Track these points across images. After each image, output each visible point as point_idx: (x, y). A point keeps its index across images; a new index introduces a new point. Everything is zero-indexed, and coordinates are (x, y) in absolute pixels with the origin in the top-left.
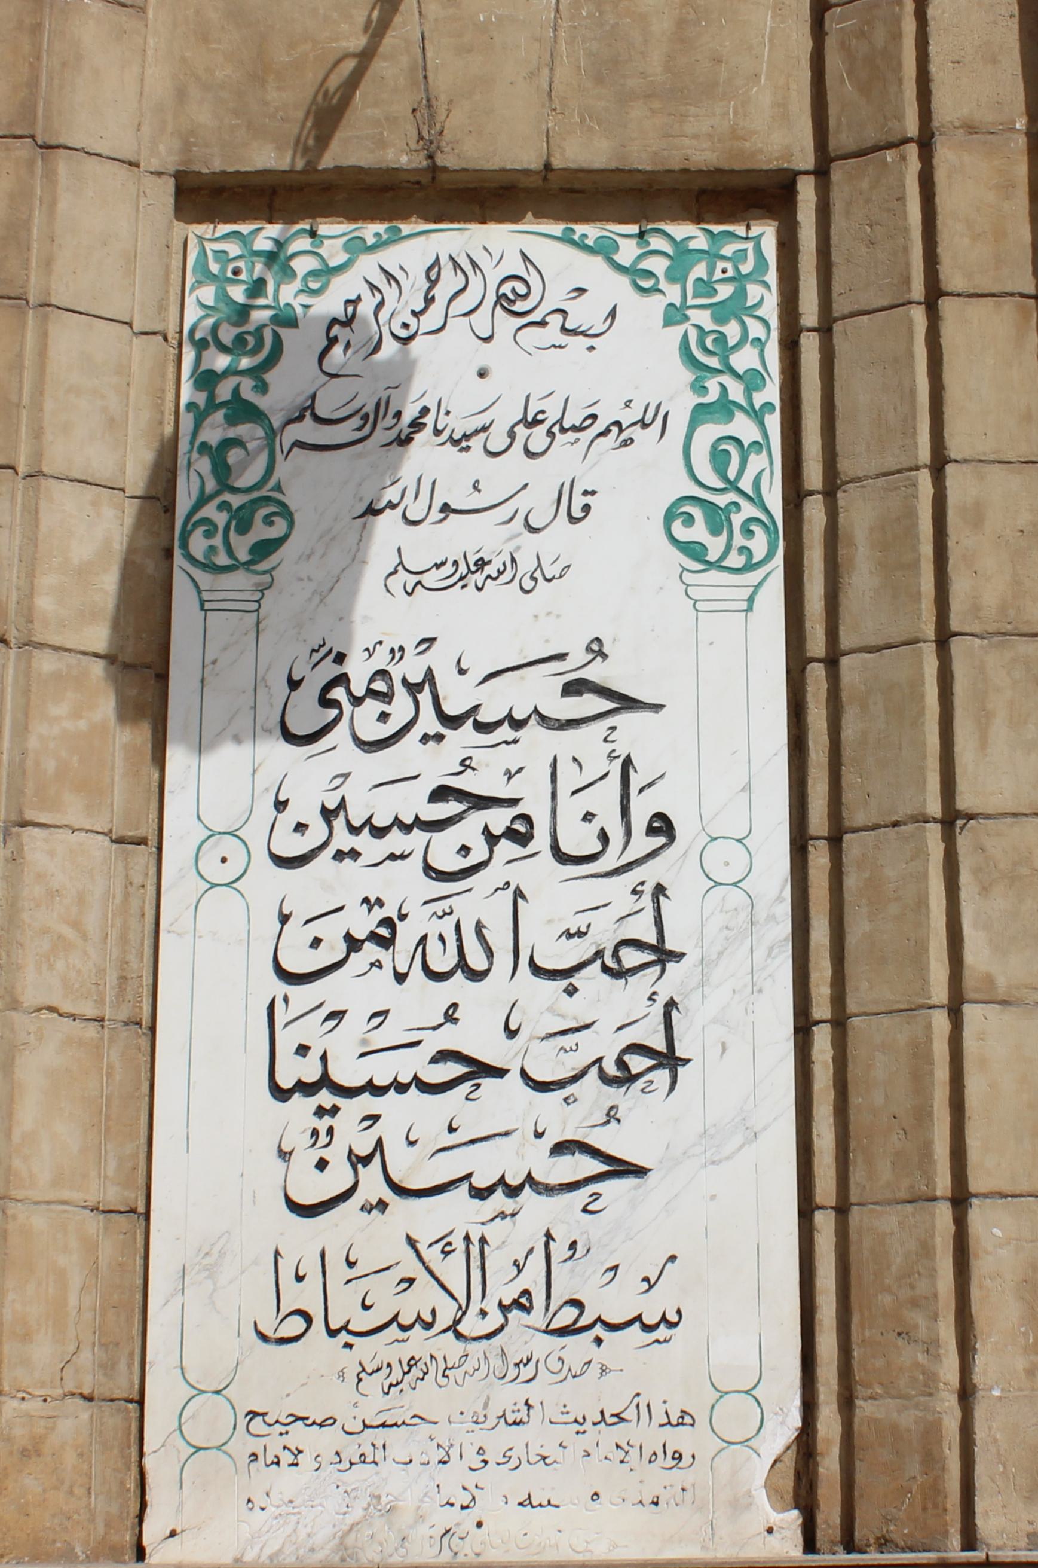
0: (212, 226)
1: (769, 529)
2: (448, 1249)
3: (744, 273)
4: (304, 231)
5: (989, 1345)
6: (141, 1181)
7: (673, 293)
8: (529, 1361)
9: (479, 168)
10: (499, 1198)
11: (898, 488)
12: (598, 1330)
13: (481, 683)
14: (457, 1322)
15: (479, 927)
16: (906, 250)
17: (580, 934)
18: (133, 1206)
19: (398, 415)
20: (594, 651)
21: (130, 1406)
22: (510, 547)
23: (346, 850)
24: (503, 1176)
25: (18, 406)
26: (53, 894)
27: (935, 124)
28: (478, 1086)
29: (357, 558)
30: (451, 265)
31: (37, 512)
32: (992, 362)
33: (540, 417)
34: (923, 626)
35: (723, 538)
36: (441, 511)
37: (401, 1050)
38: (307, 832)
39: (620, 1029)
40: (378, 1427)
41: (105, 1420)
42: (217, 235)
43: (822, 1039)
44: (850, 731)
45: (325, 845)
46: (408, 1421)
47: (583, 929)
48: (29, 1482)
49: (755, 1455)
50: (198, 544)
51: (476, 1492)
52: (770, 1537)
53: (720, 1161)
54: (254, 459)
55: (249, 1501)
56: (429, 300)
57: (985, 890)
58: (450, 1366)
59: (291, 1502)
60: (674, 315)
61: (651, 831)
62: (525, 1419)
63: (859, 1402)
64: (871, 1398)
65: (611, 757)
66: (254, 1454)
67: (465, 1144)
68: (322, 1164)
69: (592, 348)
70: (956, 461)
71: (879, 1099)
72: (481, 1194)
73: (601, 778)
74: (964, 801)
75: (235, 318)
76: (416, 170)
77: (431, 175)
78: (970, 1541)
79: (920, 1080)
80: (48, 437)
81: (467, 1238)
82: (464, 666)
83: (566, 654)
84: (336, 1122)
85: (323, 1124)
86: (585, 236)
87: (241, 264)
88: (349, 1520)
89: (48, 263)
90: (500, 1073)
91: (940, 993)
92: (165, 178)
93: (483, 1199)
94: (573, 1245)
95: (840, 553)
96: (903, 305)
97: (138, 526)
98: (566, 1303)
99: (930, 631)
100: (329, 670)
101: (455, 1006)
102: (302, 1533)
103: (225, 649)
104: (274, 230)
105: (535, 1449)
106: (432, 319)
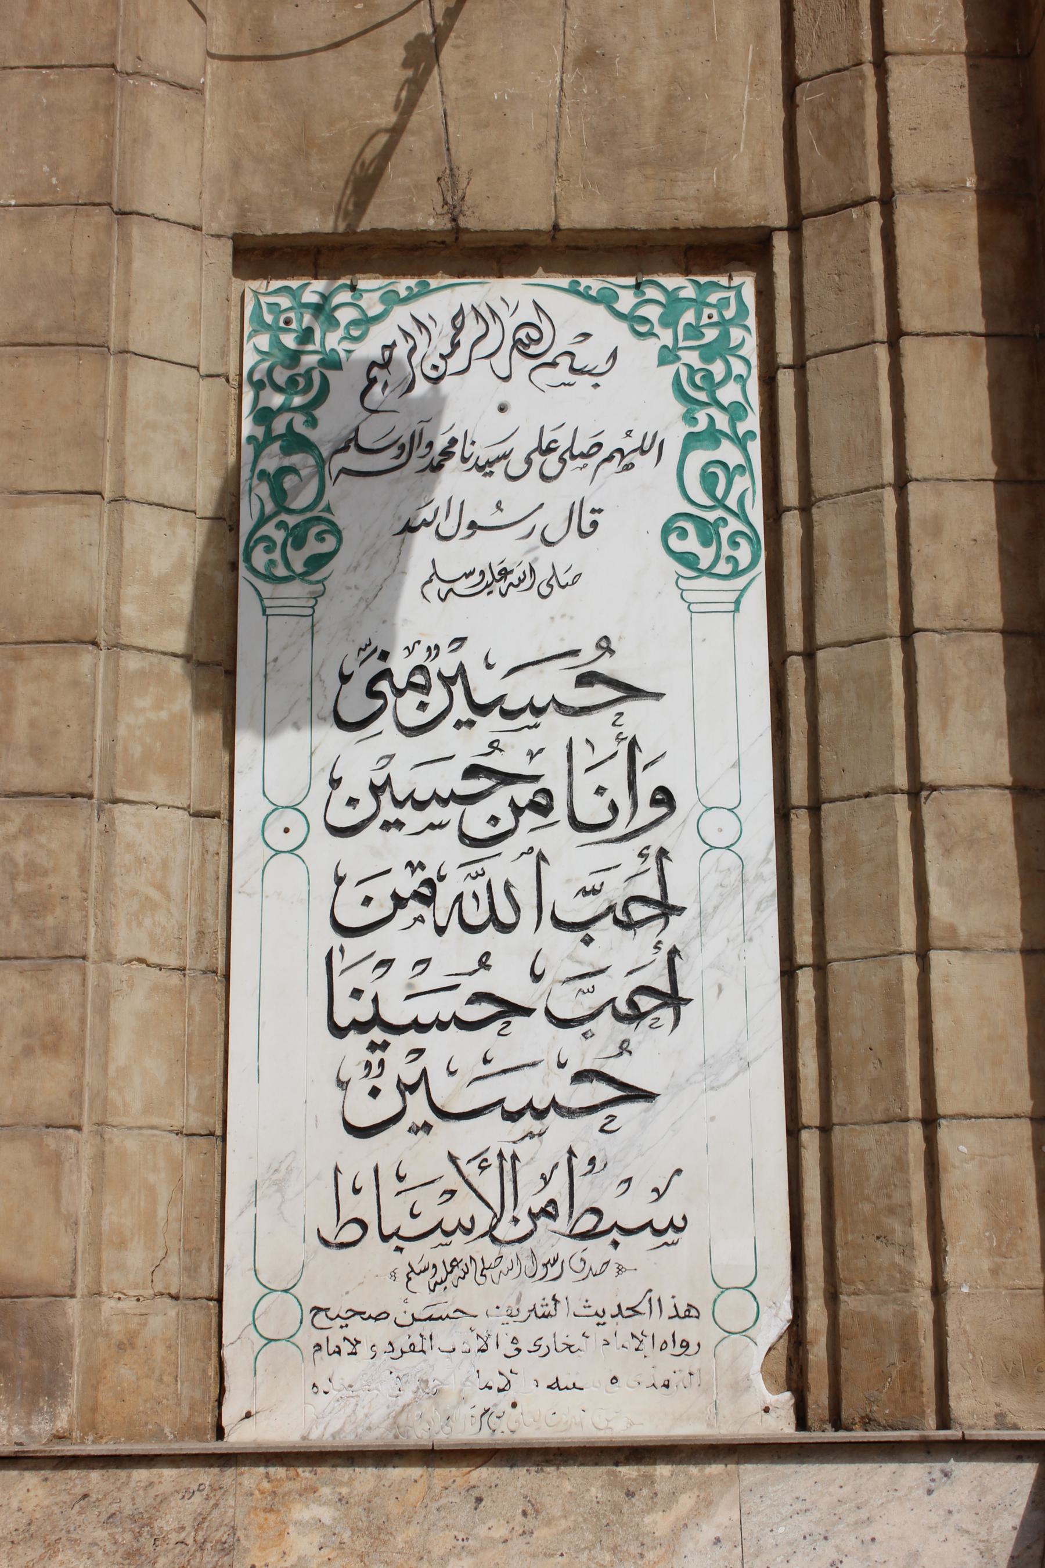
0: (265, 282)
1: (753, 541)
2: (484, 1164)
3: (727, 318)
4: (345, 285)
5: (958, 1248)
6: (218, 1108)
7: (666, 337)
8: (555, 1261)
9: (495, 229)
10: (527, 1122)
11: (866, 504)
12: (615, 1234)
13: (505, 676)
14: (493, 1228)
15: (508, 887)
16: (870, 295)
17: (595, 892)
18: (212, 1130)
19: (430, 445)
20: (603, 648)
21: (211, 1303)
22: (529, 558)
23: (392, 821)
24: (531, 1100)
25: (103, 439)
26: (141, 861)
27: (895, 184)
28: (509, 1023)
29: (397, 569)
30: (473, 314)
31: (121, 531)
32: (948, 392)
33: (553, 446)
34: (890, 624)
35: (713, 548)
36: (469, 528)
37: (442, 993)
38: (358, 806)
39: (630, 973)
40: (425, 1320)
41: (188, 1317)
42: (270, 289)
43: (805, 981)
44: (826, 715)
45: (374, 816)
46: (451, 1315)
47: (597, 887)
48: (123, 1371)
49: (752, 1344)
50: (260, 558)
51: (511, 1376)
52: (766, 1416)
53: (719, 1087)
54: (307, 483)
55: (314, 1385)
56: (455, 345)
57: (947, 852)
58: (487, 1266)
59: (351, 1386)
60: (667, 356)
61: (654, 802)
62: (553, 1313)
63: (843, 1298)
64: (854, 1294)
65: (619, 739)
66: (318, 1345)
67: (498, 1073)
68: (375, 1092)
69: (596, 385)
70: (917, 480)
71: (856, 1032)
72: (512, 1117)
73: (611, 757)
74: (929, 774)
75: (288, 362)
76: (440, 231)
77: (454, 236)
78: (944, 1421)
79: (893, 1016)
80: (130, 466)
81: (501, 1155)
82: (491, 661)
83: (580, 650)
84: (388, 1055)
85: (375, 1058)
86: (589, 287)
87: (292, 315)
88: (401, 1402)
89: (126, 315)
90: (527, 1012)
91: (909, 940)
92: (224, 240)
93: (514, 1120)
94: (592, 1161)
95: (815, 561)
96: (868, 344)
97: (208, 542)
98: (587, 1211)
99: (895, 627)
100: (375, 666)
101: (487, 954)
102: (361, 1413)
103: (285, 648)
104: (320, 285)
105: (561, 1339)
106: (458, 362)
